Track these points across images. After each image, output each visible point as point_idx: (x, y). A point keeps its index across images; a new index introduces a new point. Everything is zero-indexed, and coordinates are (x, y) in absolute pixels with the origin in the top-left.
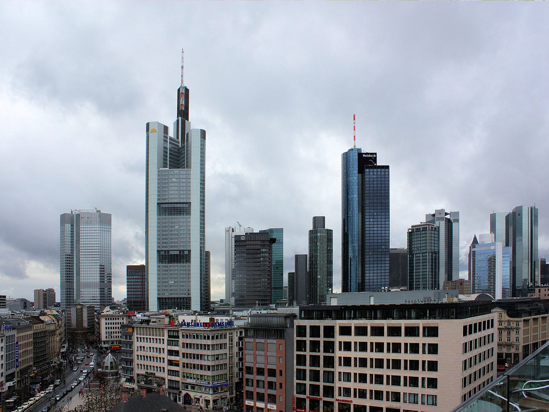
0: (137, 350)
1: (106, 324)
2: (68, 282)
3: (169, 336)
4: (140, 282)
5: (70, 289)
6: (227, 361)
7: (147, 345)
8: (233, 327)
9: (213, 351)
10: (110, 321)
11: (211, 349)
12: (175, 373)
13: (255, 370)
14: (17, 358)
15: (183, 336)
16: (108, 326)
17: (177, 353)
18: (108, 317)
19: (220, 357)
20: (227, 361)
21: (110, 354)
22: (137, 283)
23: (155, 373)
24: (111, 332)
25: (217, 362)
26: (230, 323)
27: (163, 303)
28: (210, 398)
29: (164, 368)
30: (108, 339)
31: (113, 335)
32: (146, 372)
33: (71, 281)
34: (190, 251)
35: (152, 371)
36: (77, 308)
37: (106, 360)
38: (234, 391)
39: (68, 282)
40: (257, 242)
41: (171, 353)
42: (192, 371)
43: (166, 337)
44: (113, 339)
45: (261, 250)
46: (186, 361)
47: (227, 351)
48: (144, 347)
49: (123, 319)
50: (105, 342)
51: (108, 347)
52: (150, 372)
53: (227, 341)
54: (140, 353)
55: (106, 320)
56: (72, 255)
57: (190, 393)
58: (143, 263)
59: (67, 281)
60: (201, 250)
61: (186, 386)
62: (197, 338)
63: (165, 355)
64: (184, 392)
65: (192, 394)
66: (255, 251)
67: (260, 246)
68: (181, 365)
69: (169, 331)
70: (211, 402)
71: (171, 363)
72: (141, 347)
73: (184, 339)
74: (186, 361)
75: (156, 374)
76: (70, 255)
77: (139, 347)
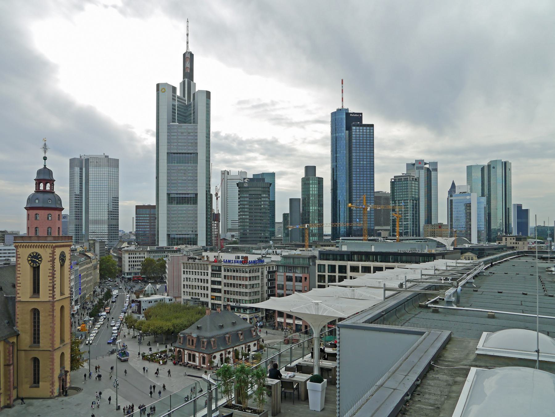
0: (184, 281)
1: (129, 258)
2: (77, 219)
3: (212, 270)
4: (148, 220)
5: (79, 225)
6: (260, 289)
7: (193, 277)
8: (263, 264)
9: (250, 282)
10: (133, 256)
11: (248, 280)
12: (219, 298)
14: (80, 287)
15: (225, 271)
16: (131, 260)
17: (219, 283)
18: (130, 252)
19: (255, 286)
20: (260, 289)
21: (150, 284)
22: (145, 221)
23: (199, 299)
24: (134, 265)
25: (253, 290)
26: (260, 261)
27: (171, 240)
28: (247, 316)
29: (207, 294)
30: (130, 271)
31: (135, 267)
32: (191, 298)
33: (79, 218)
34: (196, 194)
35: (197, 297)
36: (89, 243)
37: (146, 289)
39: (77, 219)
40: (258, 188)
41: (213, 283)
42: (233, 297)
43: (210, 271)
44: (135, 271)
45: (262, 195)
46: (227, 289)
47: (259, 282)
48: (190, 278)
49: (144, 254)
50: (128, 274)
51: (131, 278)
52: (195, 297)
53: (260, 274)
54: (186, 283)
55: (129, 254)
56: (81, 195)
58: (154, 203)
59: (76, 218)
60: (207, 194)
62: (237, 271)
63: (209, 285)
66: (256, 196)
67: (260, 192)
68: (223, 292)
69: (212, 266)
70: (248, 320)
71: (213, 290)
72: (187, 278)
73: (226, 272)
74: (227, 289)
75: (200, 299)
76: (79, 195)
77: (185, 278)
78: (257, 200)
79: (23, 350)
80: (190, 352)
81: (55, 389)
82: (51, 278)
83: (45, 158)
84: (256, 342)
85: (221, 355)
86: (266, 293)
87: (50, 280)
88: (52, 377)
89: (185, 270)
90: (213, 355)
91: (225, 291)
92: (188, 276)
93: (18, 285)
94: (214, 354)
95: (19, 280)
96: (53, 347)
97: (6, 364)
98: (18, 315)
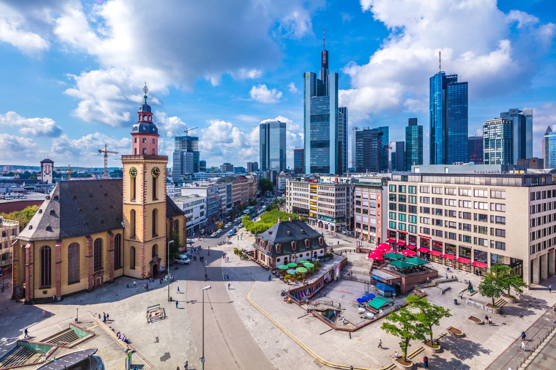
3: (311, 188)
7: (299, 192)
13: (362, 211)
19: (341, 201)
27: (314, 169)
28: (334, 225)
38: (350, 222)
43: (309, 189)
53: (345, 192)
57: (322, 221)
61: (320, 216)
64: (319, 220)
65: (324, 222)
78: (368, 143)
84: (323, 249)
89: (295, 187)
90: (277, 259)
91: (319, 204)
92: (296, 192)
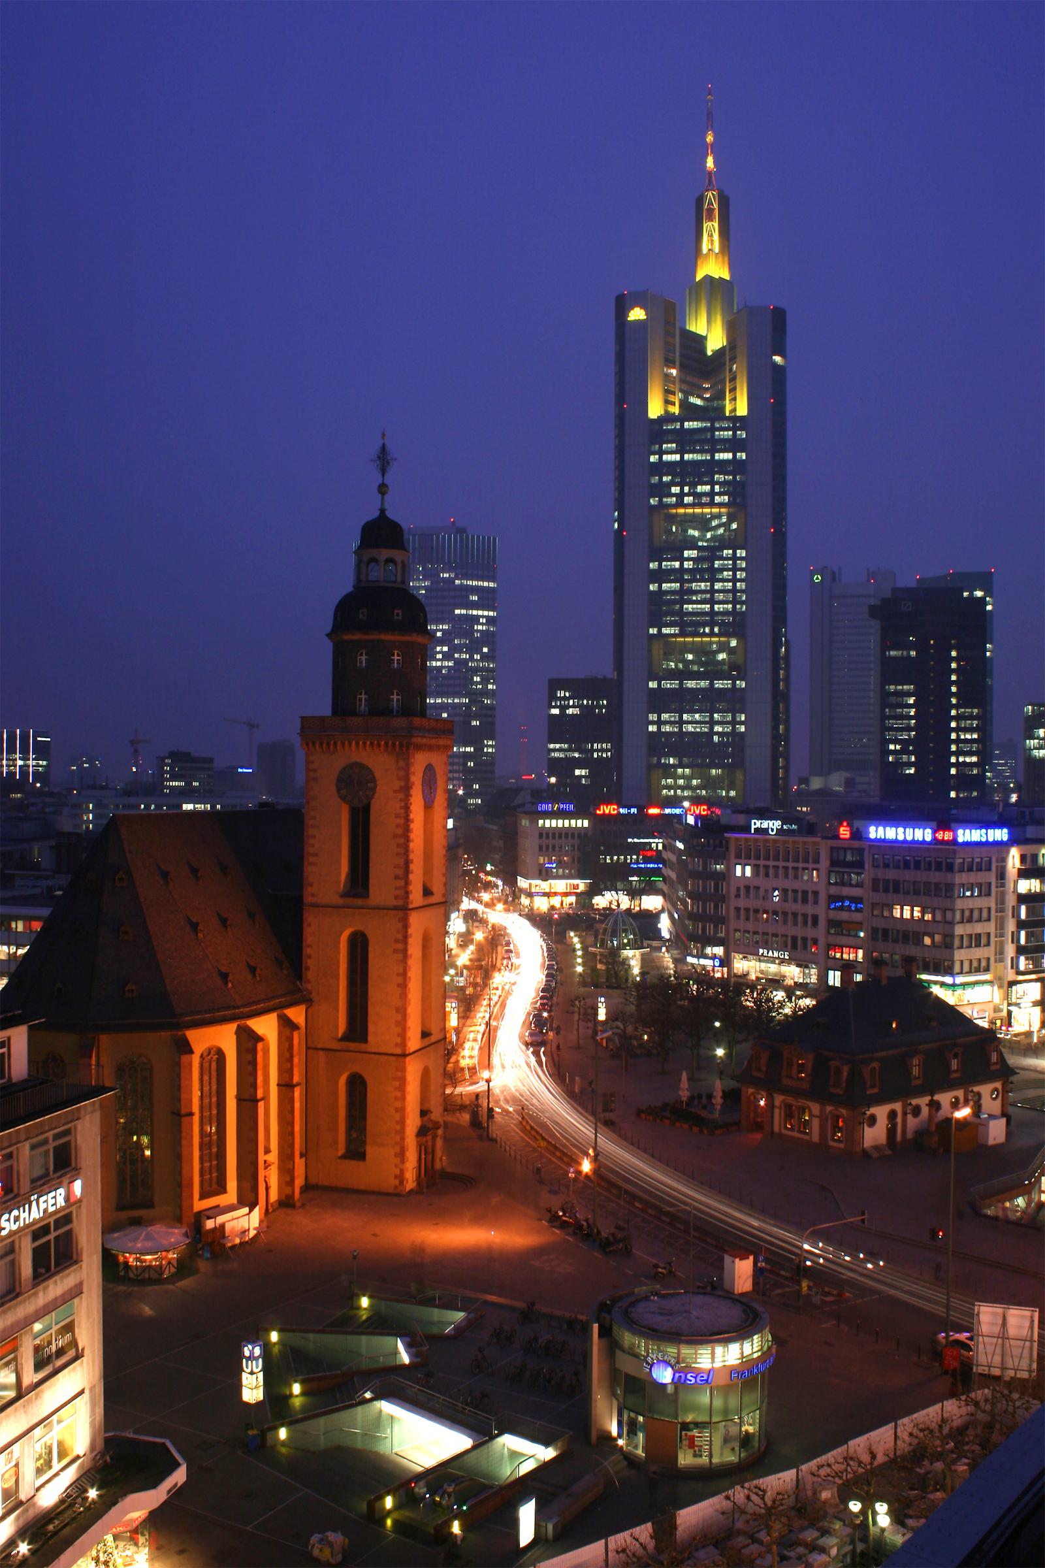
0: (738, 896)
54: (742, 903)
63: (821, 910)
79: (322, 1049)
80: (791, 1100)
81: (407, 1169)
82: (402, 841)
83: (383, 489)
84: (998, 1085)
85: (892, 1115)
86: (1013, 942)
87: (398, 846)
88: (402, 1132)
90: (868, 1113)
93: (311, 859)
94: (873, 1110)
95: (313, 846)
96: (404, 1044)
97: (283, 1083)
98: (310, 946)
